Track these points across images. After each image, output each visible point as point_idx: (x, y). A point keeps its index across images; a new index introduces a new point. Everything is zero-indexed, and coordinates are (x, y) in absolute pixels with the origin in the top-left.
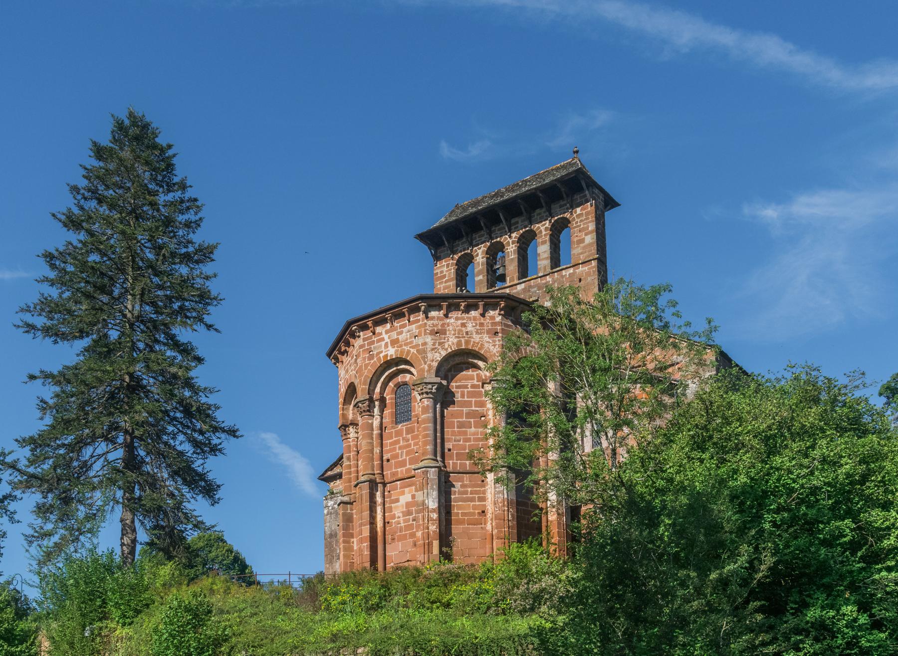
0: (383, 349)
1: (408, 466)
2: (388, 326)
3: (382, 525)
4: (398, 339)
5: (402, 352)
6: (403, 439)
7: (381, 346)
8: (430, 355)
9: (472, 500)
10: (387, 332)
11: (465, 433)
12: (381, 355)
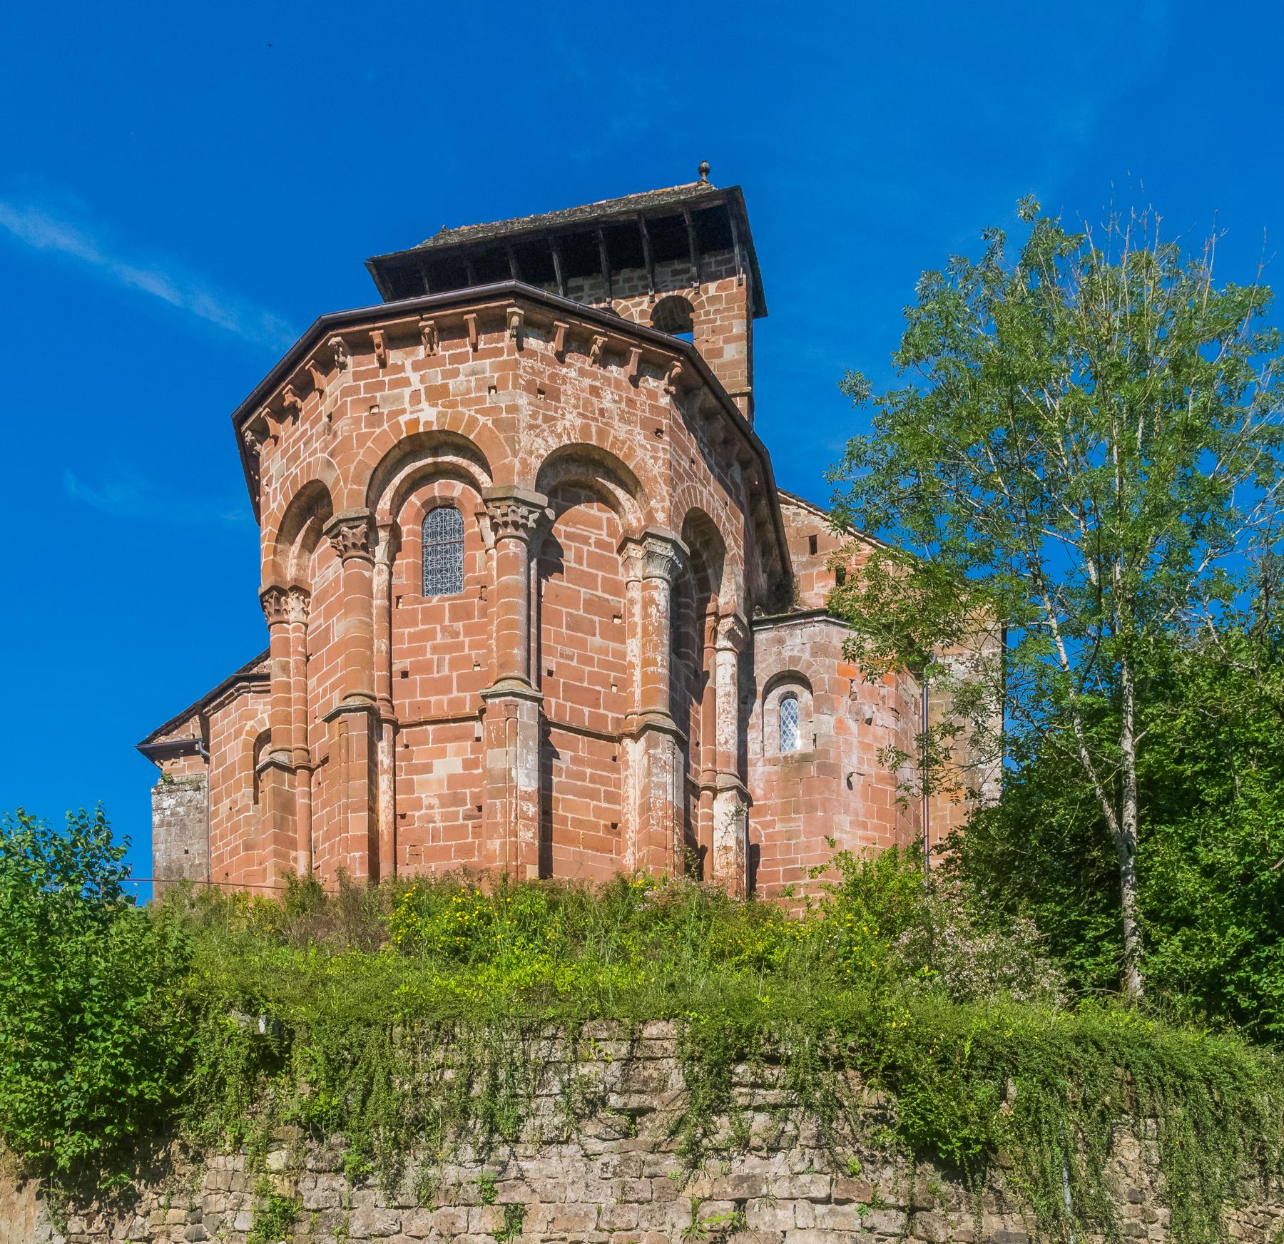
0: (406, 405)
1: (455, 694)
2: (421, 352)
3: (391, 818)
4: (445, 386)
6: (444, 629)
7: (399, 398)
9: (593, 795)
10: (417, 367)
11: (582, 644)
12: (402, 419)
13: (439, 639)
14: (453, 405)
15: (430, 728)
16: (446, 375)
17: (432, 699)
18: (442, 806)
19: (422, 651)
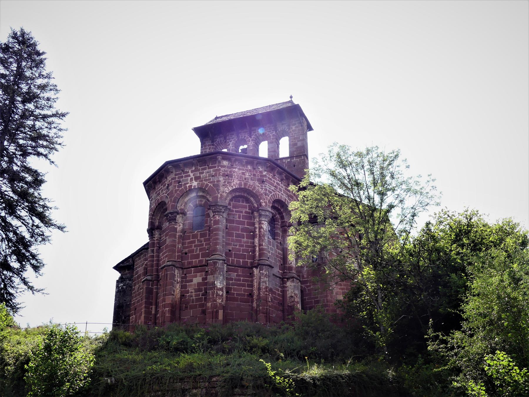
0: (189, 182)
1: (200, 259)
5: (203, 184)
6: (198, 240)
7: (188, 179)
8: (221, 189)
9: (243, 285)
10: (192, 172)
11: (240, 241)
13: (196, 243)
14: (202, 181)
15: (193, 269)
16: (200, 173)
17: (194, 260)
18: (195, 292)
19: (191, 246)
